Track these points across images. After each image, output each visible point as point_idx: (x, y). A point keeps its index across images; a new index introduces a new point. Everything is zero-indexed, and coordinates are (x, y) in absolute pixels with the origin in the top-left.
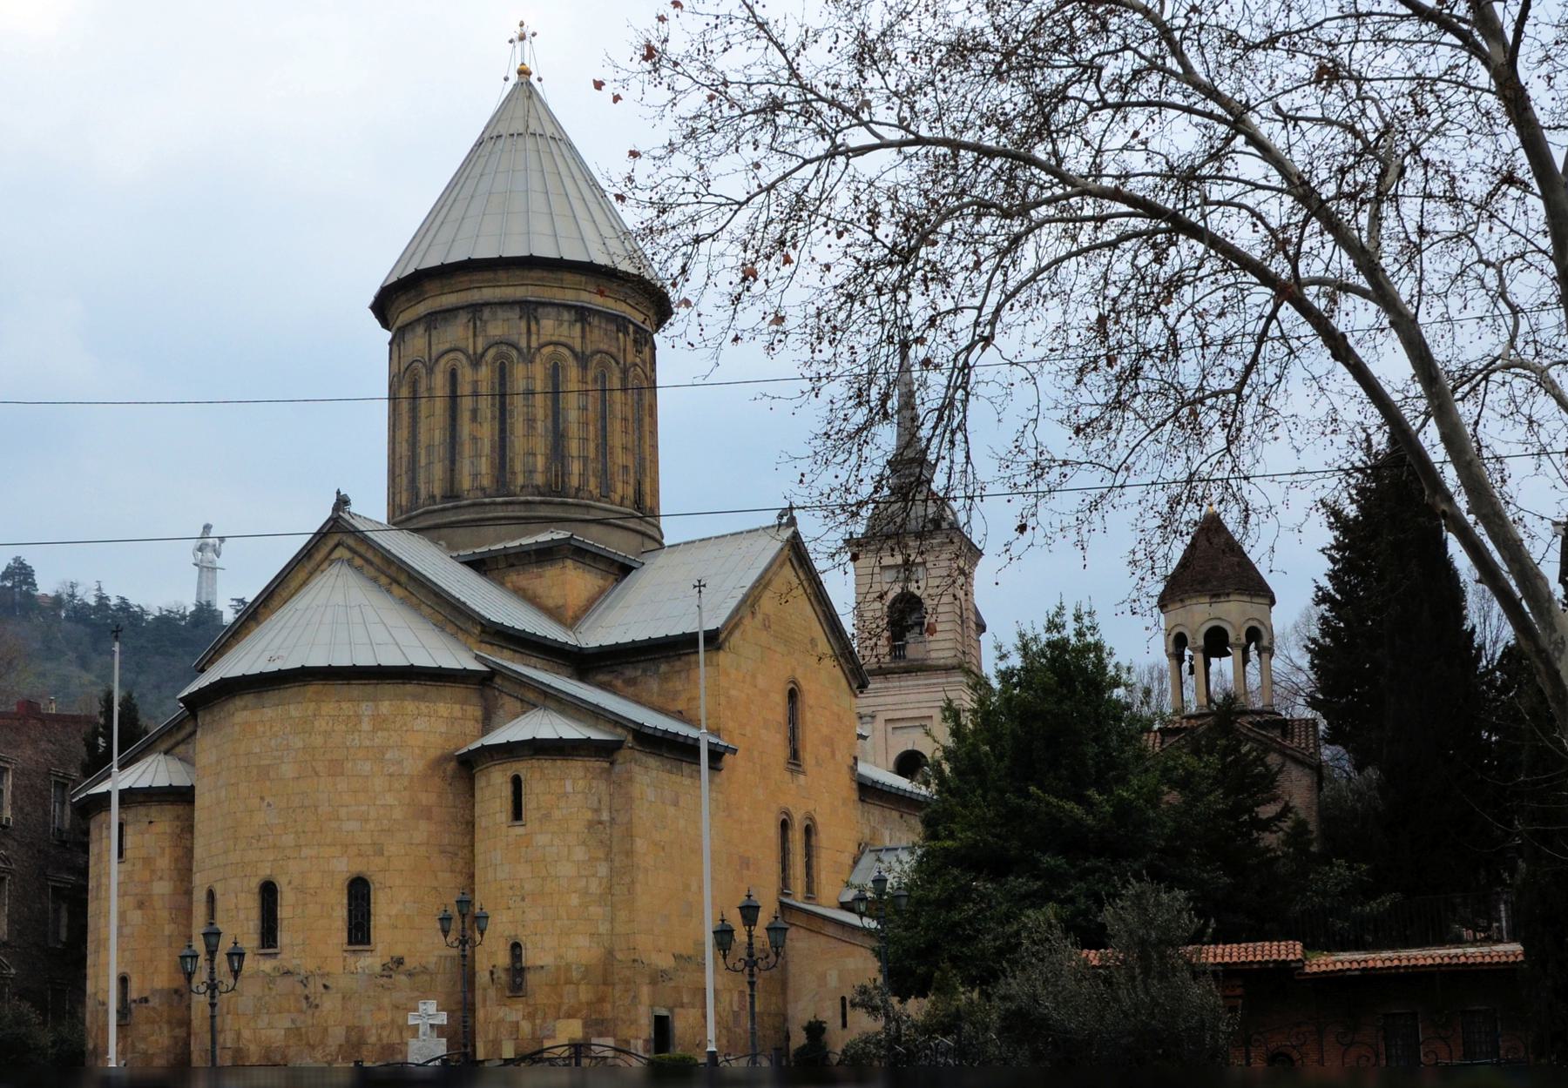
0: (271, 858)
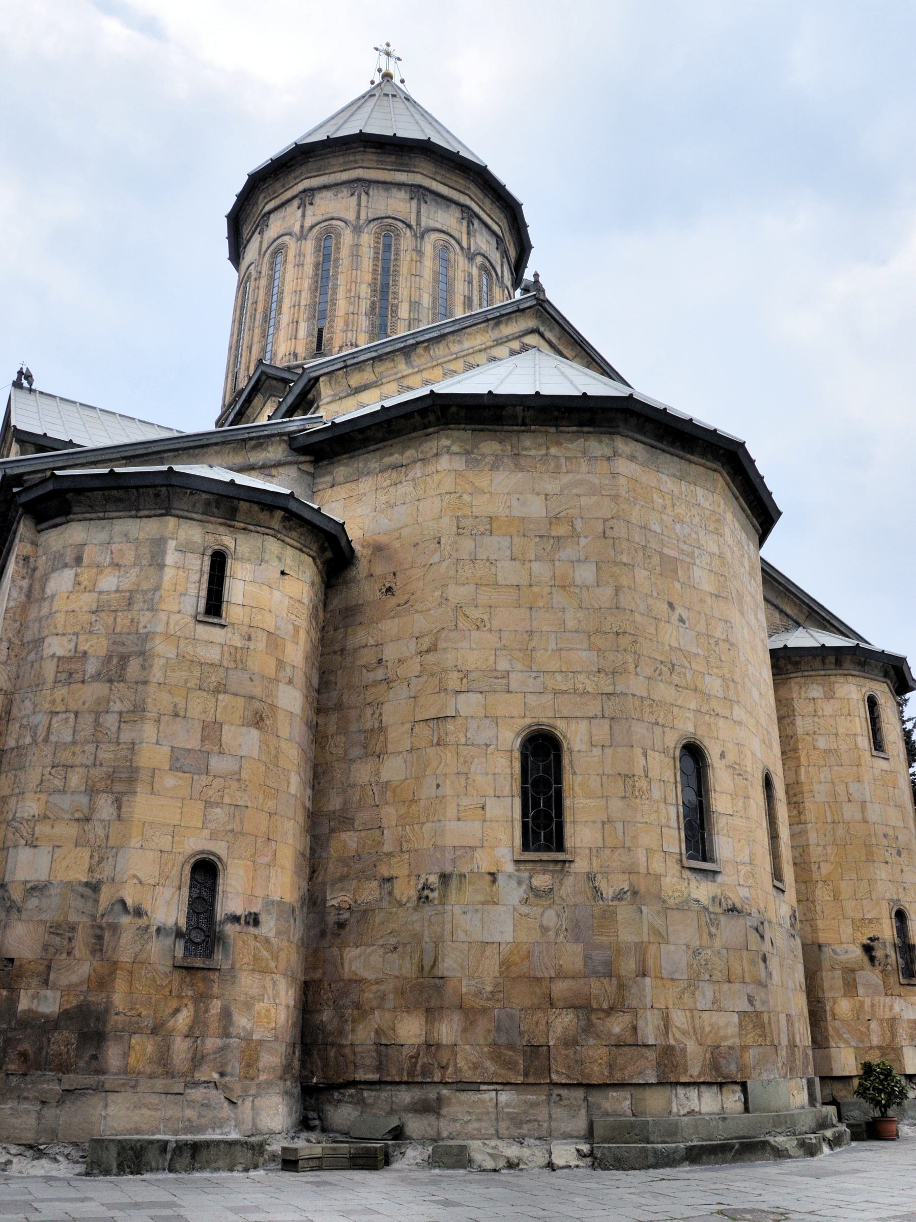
0: (693, 706)
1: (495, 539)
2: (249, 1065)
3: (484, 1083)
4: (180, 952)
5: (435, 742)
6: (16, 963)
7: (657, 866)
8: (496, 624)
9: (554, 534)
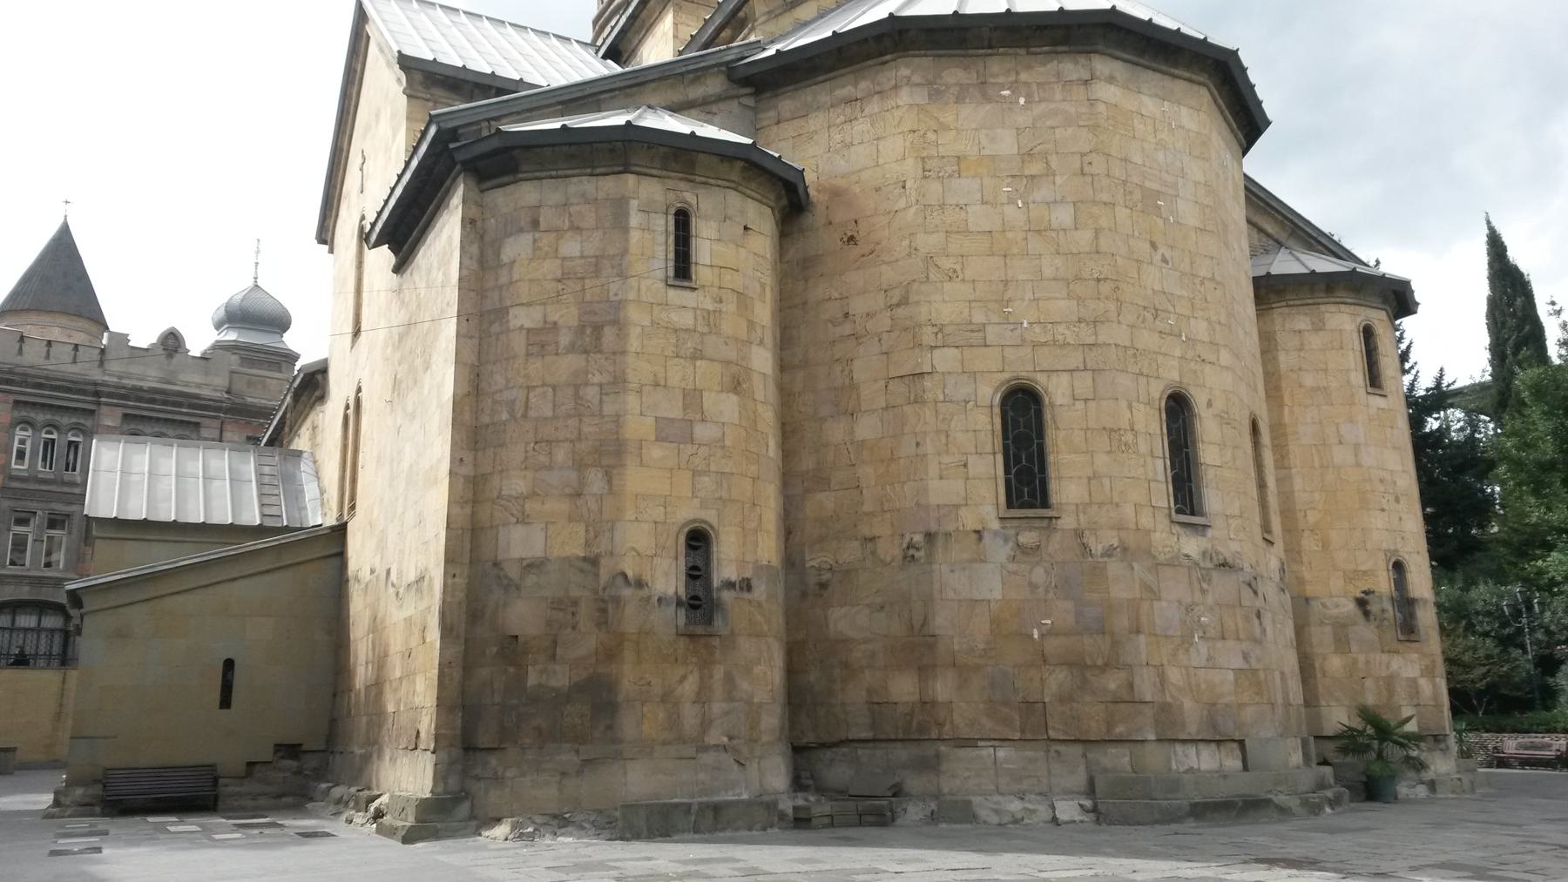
0: (1178, 353)
1: (963, 181)
2: (752, 728)
3: (982, 740)
4: (682, 621)
5: (912, 398)
6: (521, 640)
7: (1146, 521)
8: (969, 273)
9: (1027, 172)
